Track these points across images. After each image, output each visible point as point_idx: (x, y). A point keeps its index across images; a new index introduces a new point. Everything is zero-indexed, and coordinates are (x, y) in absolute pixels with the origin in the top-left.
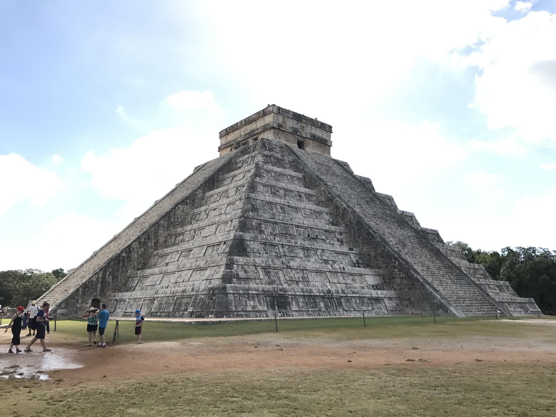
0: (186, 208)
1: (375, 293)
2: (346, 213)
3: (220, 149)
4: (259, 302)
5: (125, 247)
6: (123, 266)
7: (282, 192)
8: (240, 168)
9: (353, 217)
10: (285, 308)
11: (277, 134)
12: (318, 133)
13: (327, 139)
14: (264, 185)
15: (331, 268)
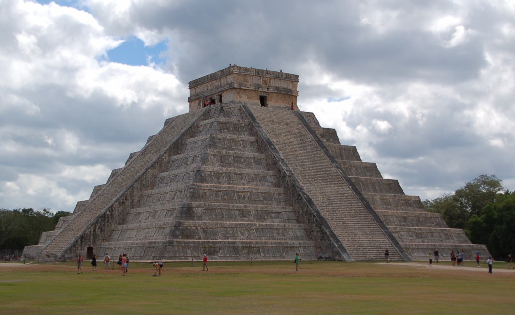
0: (155, 171)
1: (296, 242)
2: (285, 177)
3: (190, 100)
4: (196, 251)
5: (108, 206)
6: (108, 221)
7: (231, 159)
8: (201, 132)
9: (289, 181)
10: (214, 254)
11: (238, 93)
12: (283, 85)
13: (293, 89)
14: (214, 156)
15: (258, 225)
